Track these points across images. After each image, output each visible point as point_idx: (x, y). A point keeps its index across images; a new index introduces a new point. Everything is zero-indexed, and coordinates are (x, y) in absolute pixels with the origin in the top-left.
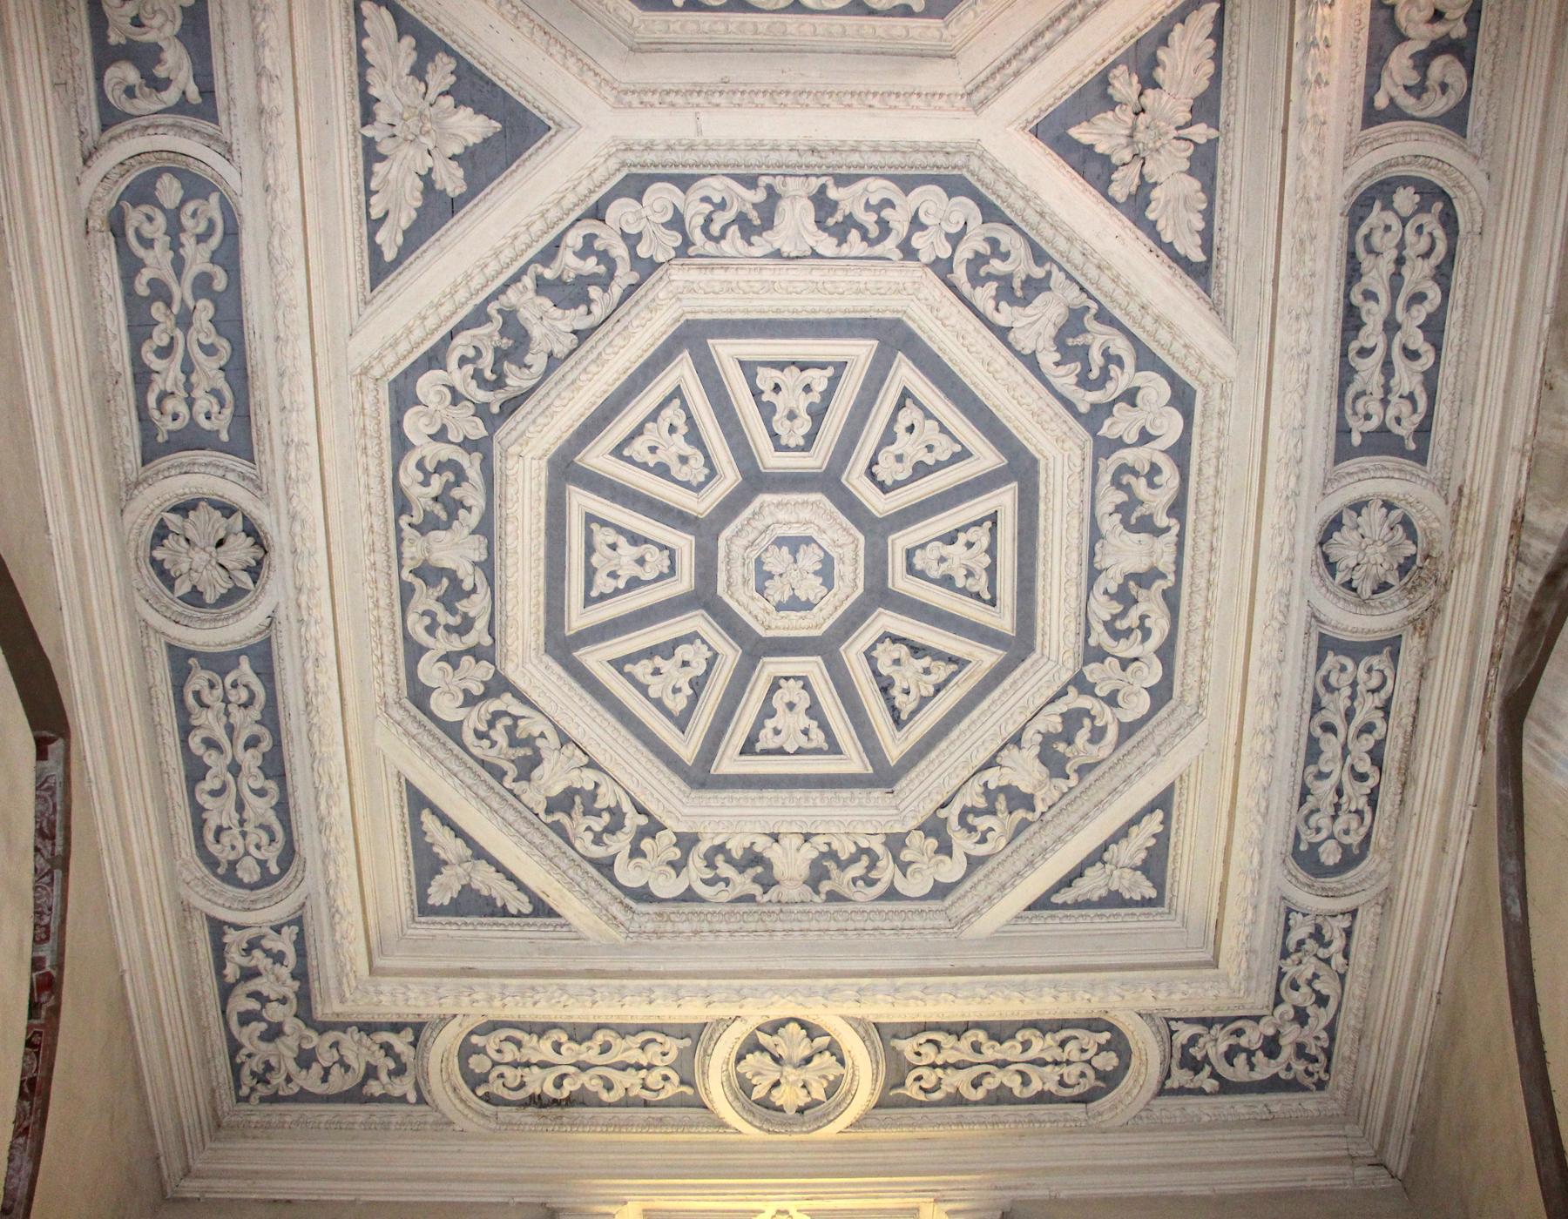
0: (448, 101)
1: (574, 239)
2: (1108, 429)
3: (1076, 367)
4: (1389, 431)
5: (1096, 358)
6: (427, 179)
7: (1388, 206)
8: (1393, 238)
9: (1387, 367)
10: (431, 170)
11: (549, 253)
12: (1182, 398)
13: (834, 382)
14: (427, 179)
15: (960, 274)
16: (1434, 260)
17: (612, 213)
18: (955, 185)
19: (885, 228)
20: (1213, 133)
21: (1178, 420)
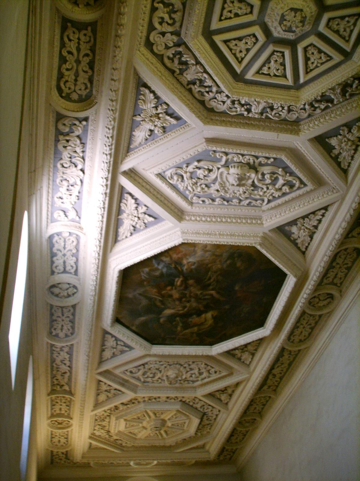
0: (336, 147)
1: (318, 111)
2: (175, 38)
3: (183, 59)
4: (77, 29)
5: (176, 61)
6: (350, 131)
7: (80, 96)
8: (77, 88)
9: (78, 50)
10: (348, 134)
11: (327, 108)
12: (149, 45)
13: (261, 69)
14: (350, 131)
15: (214, 89)
16: (64, 80)
17: (306, 115)
18: (211, 110)
19: (233, 102)
20: (134, 118)
21: (151, 39)
